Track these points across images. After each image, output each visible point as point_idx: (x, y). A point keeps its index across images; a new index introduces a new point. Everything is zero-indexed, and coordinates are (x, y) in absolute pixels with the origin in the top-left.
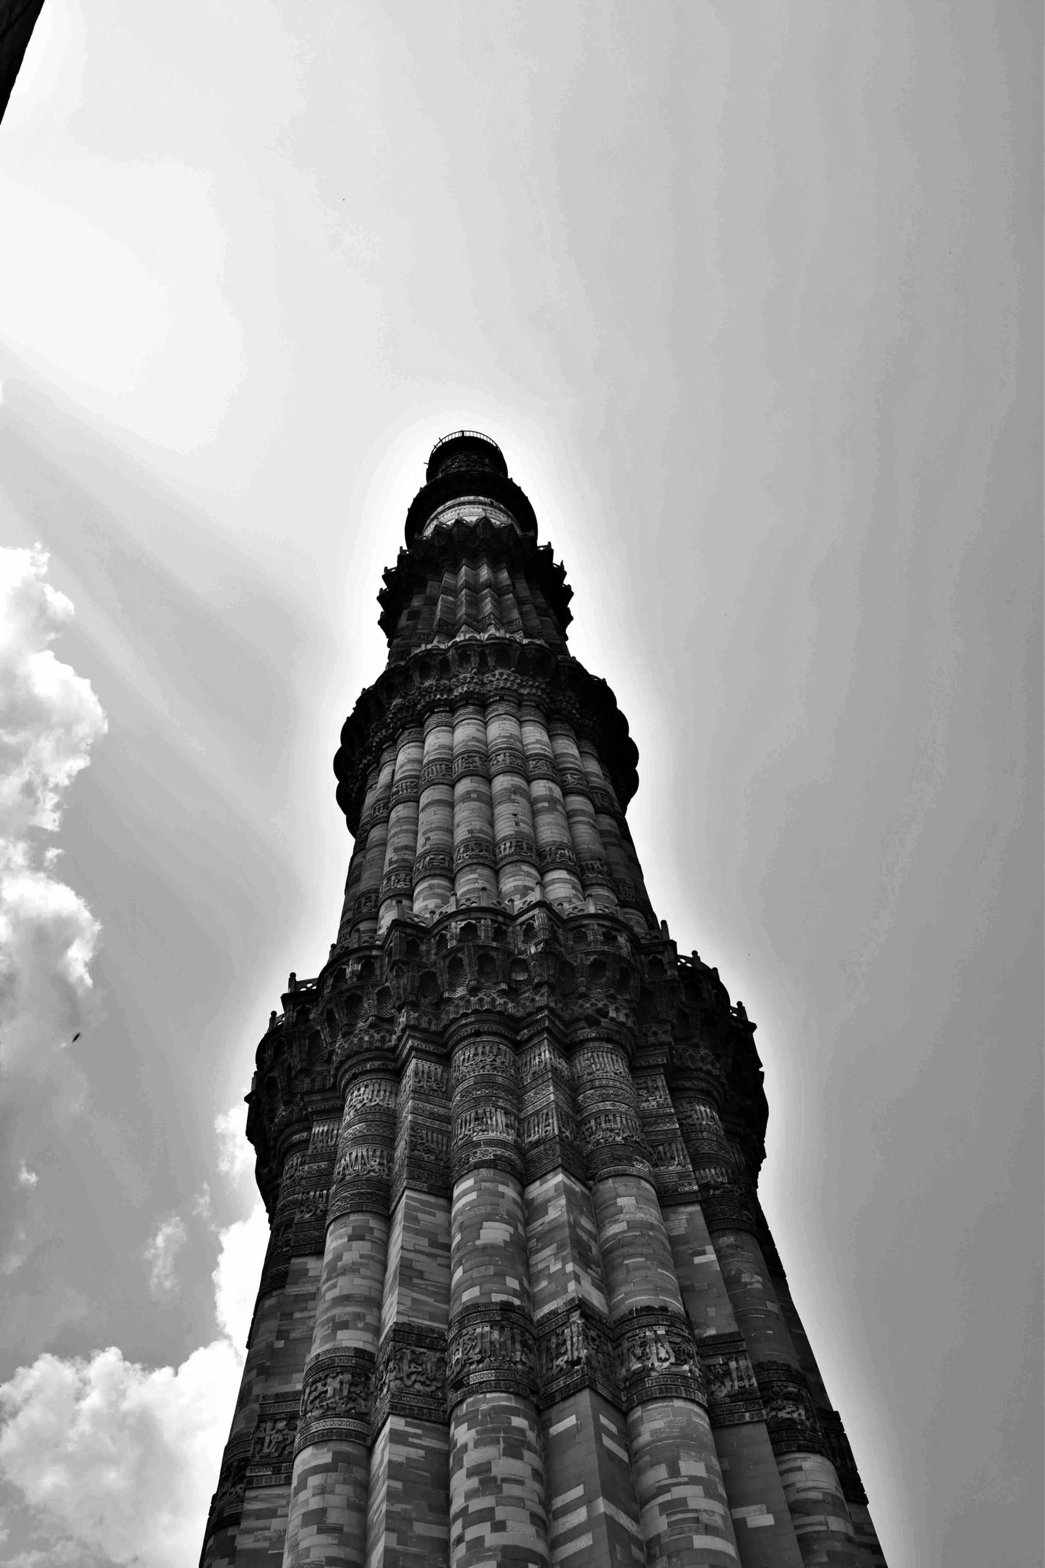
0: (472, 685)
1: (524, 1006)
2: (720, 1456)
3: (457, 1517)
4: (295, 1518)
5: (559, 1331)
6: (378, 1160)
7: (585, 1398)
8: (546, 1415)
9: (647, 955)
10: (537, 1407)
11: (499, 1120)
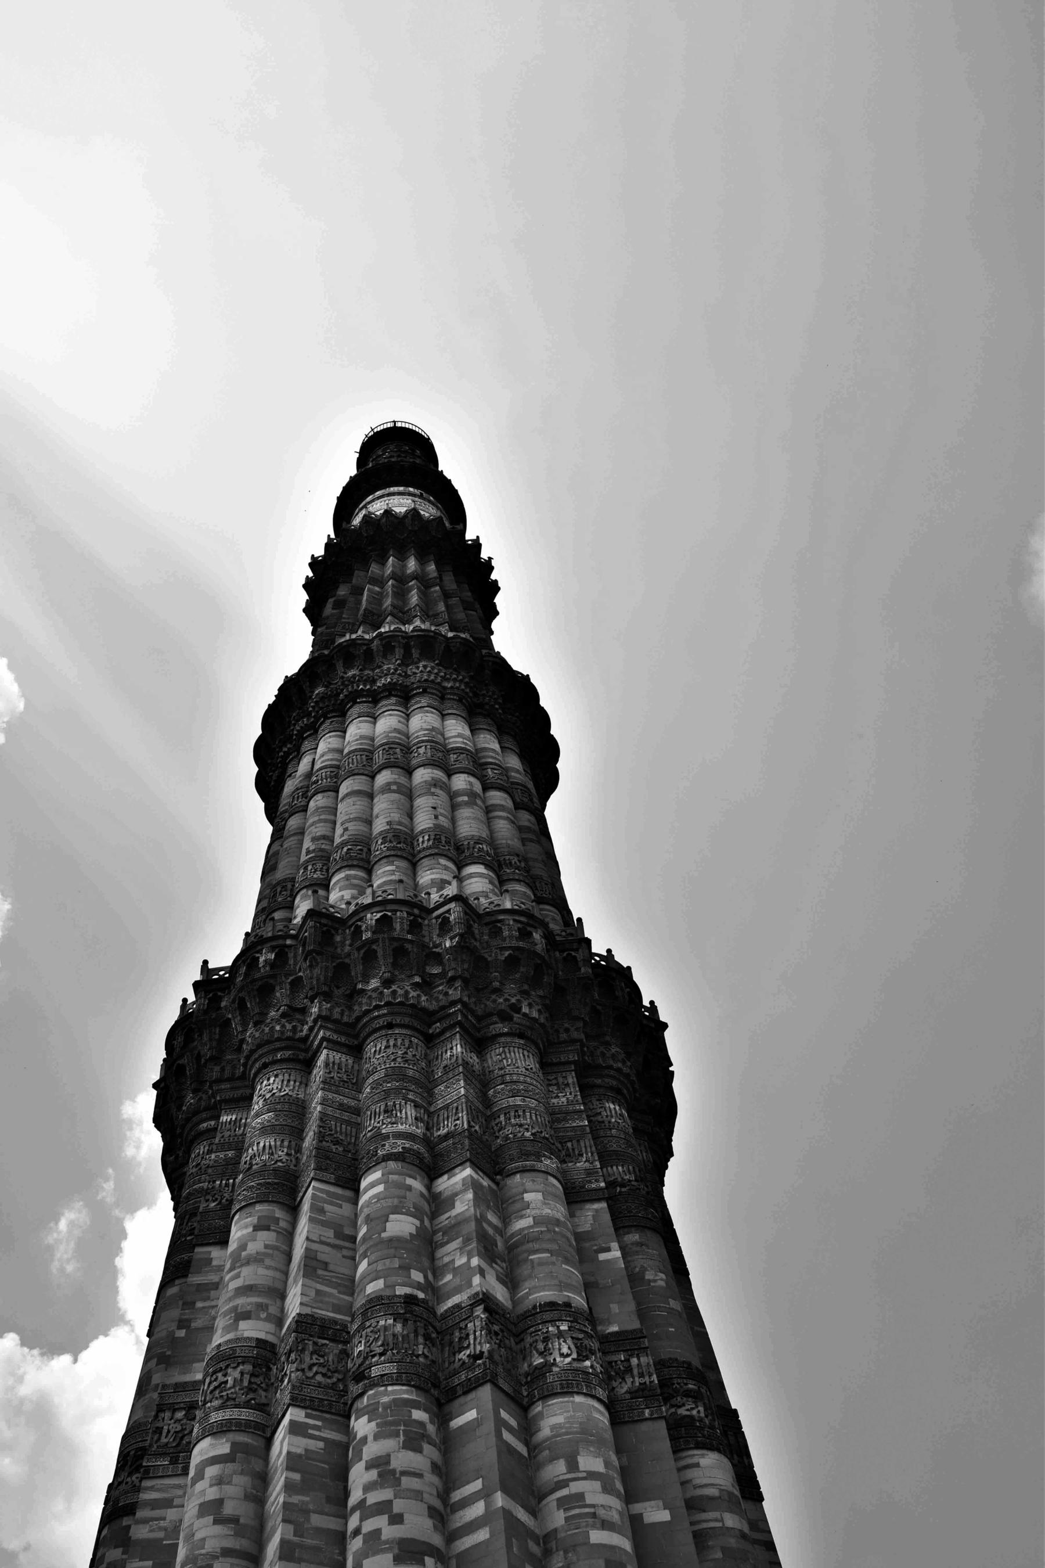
0: (396, 676)
1: (437, 1000)
2: (618, 1452)
3: (354, 1509)
4: (191, 1508)
5: (462, 1325)
6: (285, 1150)
7: (486, 1392)
9: (563, 951)
10: (438, 1400)
11: (409, 1113)
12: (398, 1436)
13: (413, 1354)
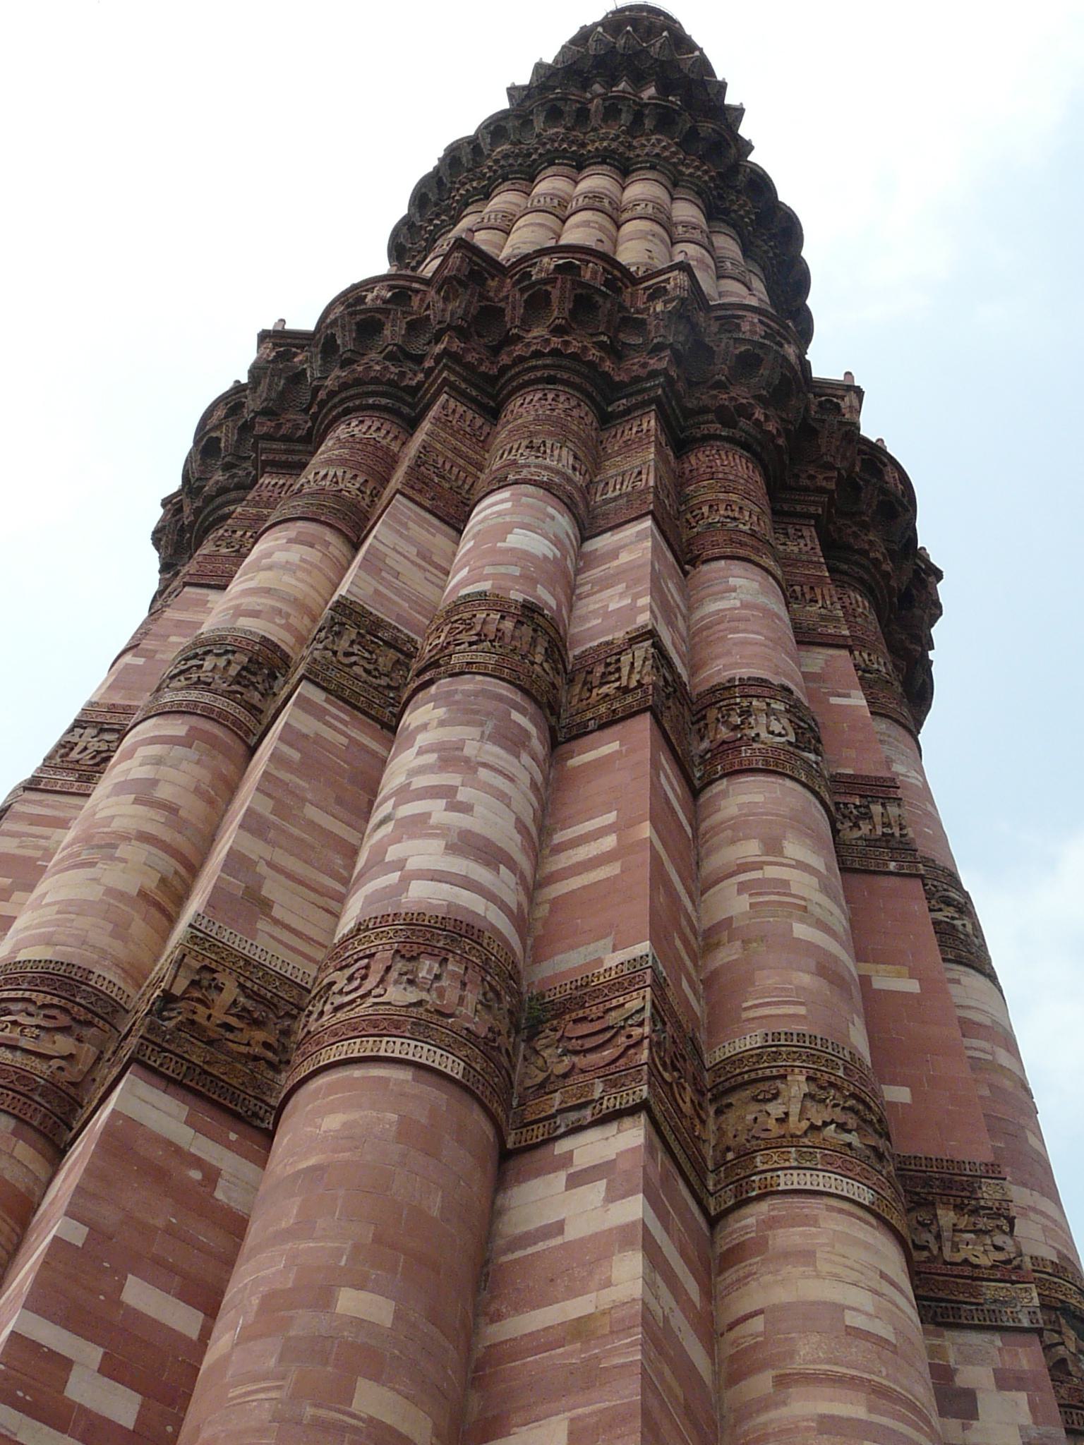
3: (386, 800)
5: (614, 658)
6: (358, 485)
7: (644, 724)
8: (567, 747)
10: (552, 731)
12: (482, 724)
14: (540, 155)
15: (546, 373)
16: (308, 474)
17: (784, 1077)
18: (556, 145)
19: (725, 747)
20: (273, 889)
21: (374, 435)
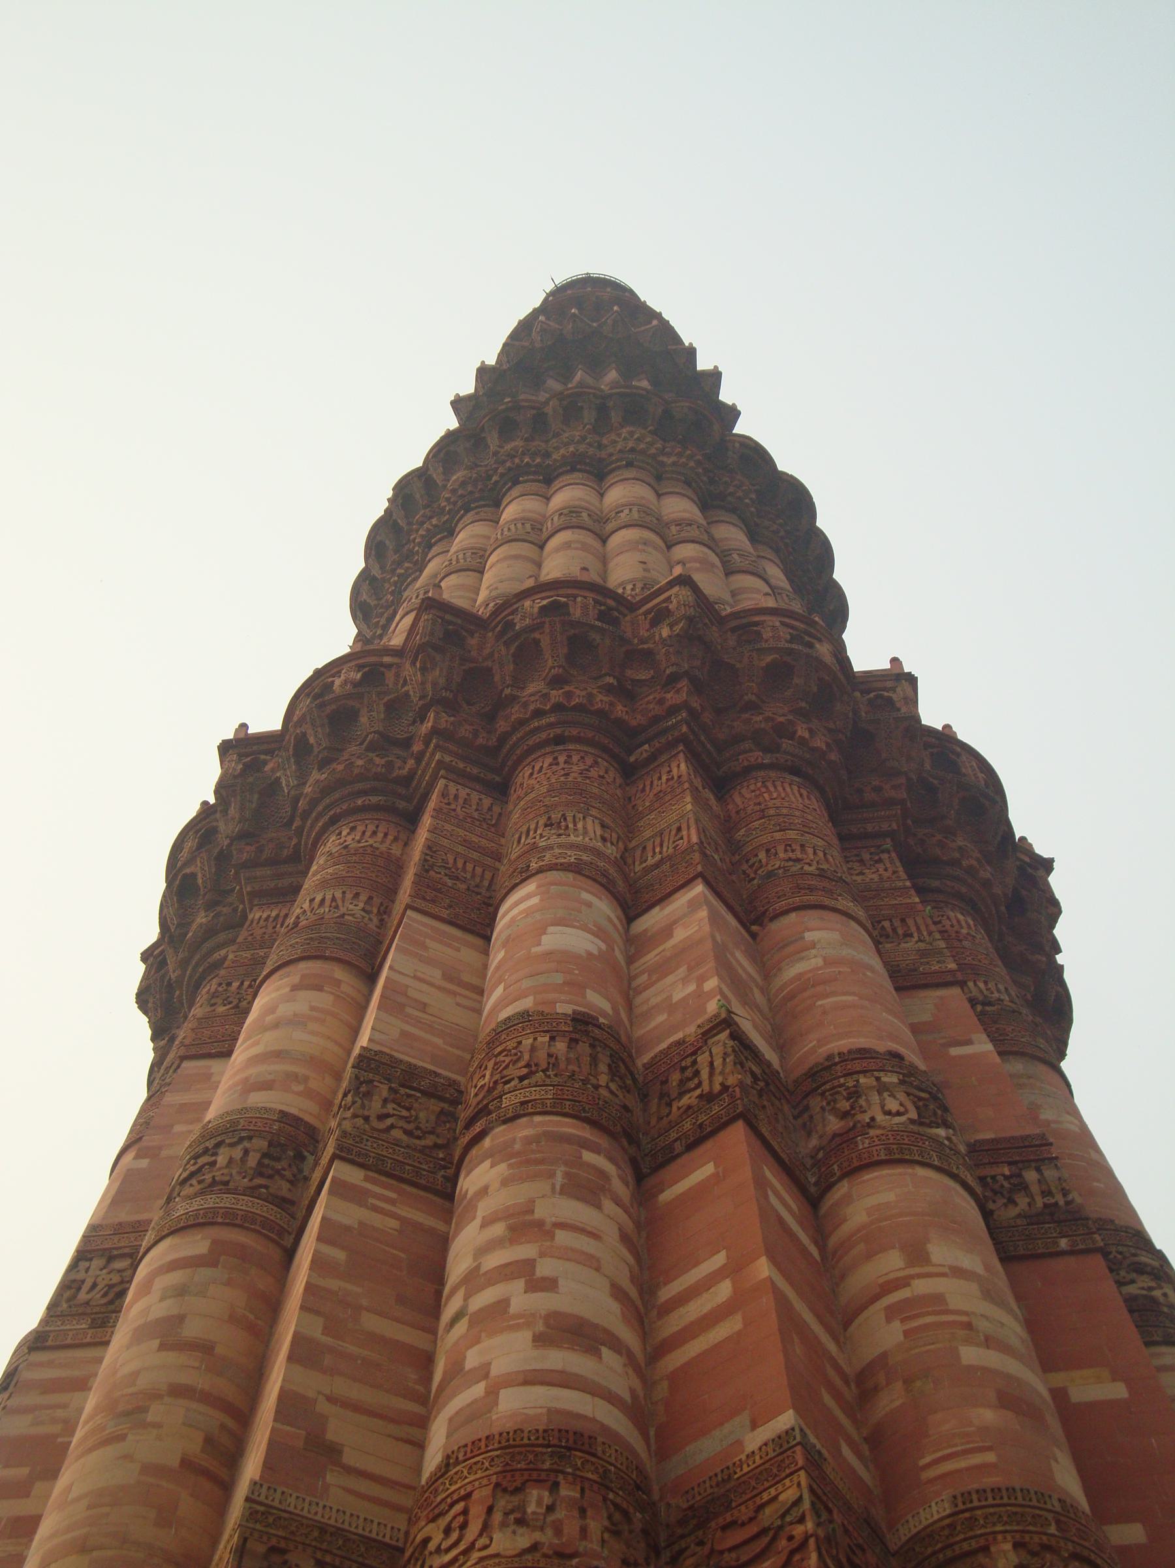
5: (689, 1060)
6: (361, 905)
7: (737, 1136)
9: (868, 692)
10: (634, 1163)
13: (585, 1082)
14: (502, 475)
15: (552, 733)
16: (302, 903)
17: (985, 1549)
18: (517, 460)
19: (838, 1140)
20: (341, 1429)
21: (371, 841)
